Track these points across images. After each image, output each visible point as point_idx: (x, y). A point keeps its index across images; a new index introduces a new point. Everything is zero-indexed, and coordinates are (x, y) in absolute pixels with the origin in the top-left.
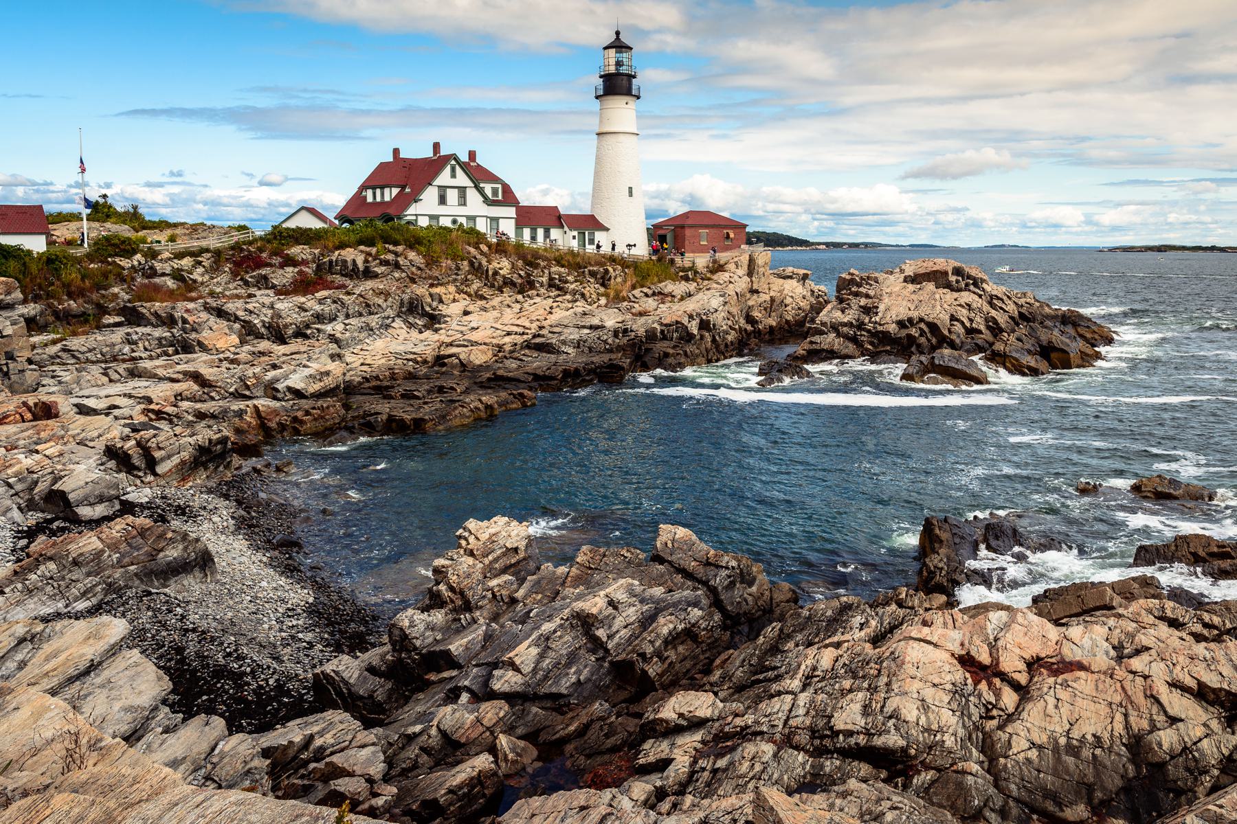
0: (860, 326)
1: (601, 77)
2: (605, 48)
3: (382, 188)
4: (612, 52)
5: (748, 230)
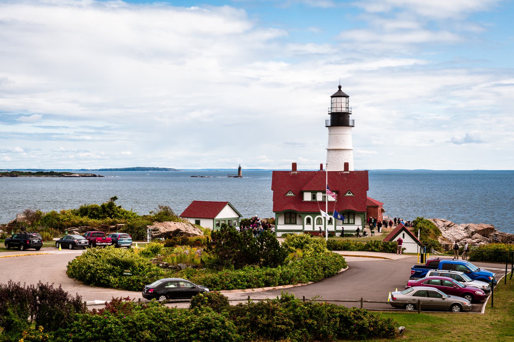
4: (344, 99)
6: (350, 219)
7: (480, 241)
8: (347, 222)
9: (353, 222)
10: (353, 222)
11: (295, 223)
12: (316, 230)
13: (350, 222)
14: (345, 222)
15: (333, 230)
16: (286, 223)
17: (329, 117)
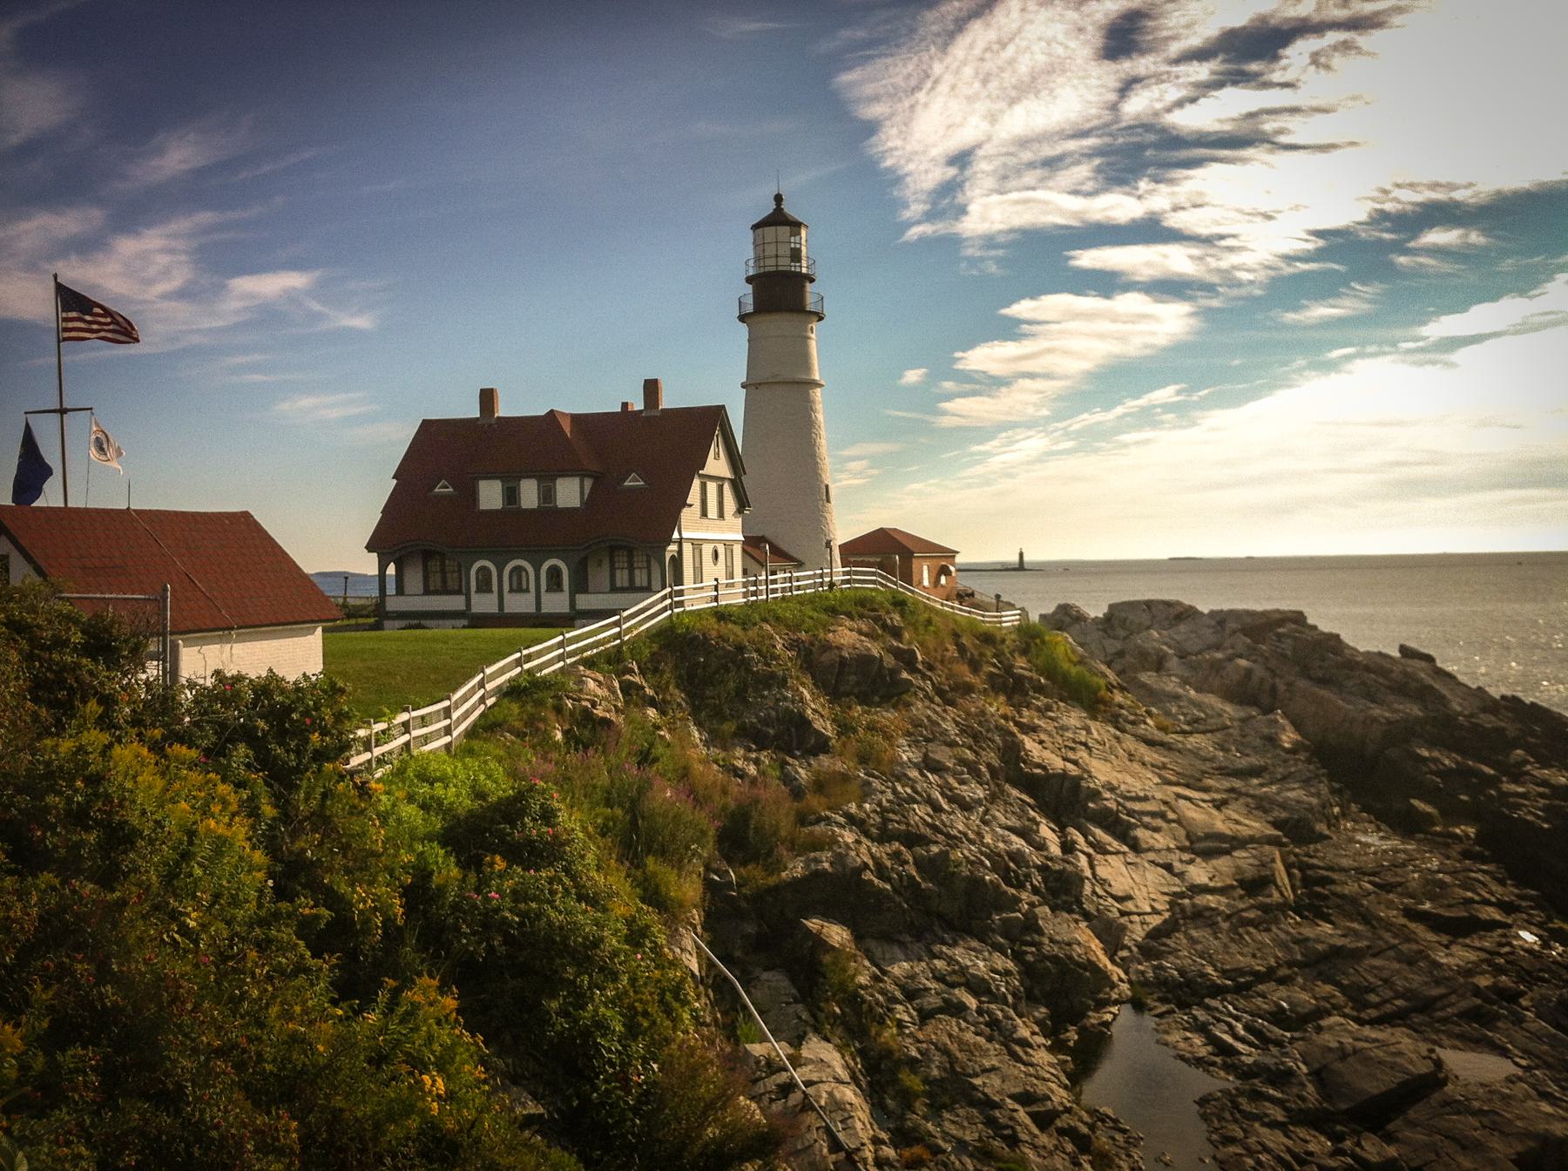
0: (1449, 720)
1: (749, 280)
2: (755, 227)
3: (547, 480)
4: (784, 231)
5: (959, 559)
6: (637, 572)
7: (1241, 656)
8: (626, 584)
9: (645, 584)
13: (638, 583)
14: (619, 584)
15: (566, 609)
16: (427, 592)
17: (749, 289)
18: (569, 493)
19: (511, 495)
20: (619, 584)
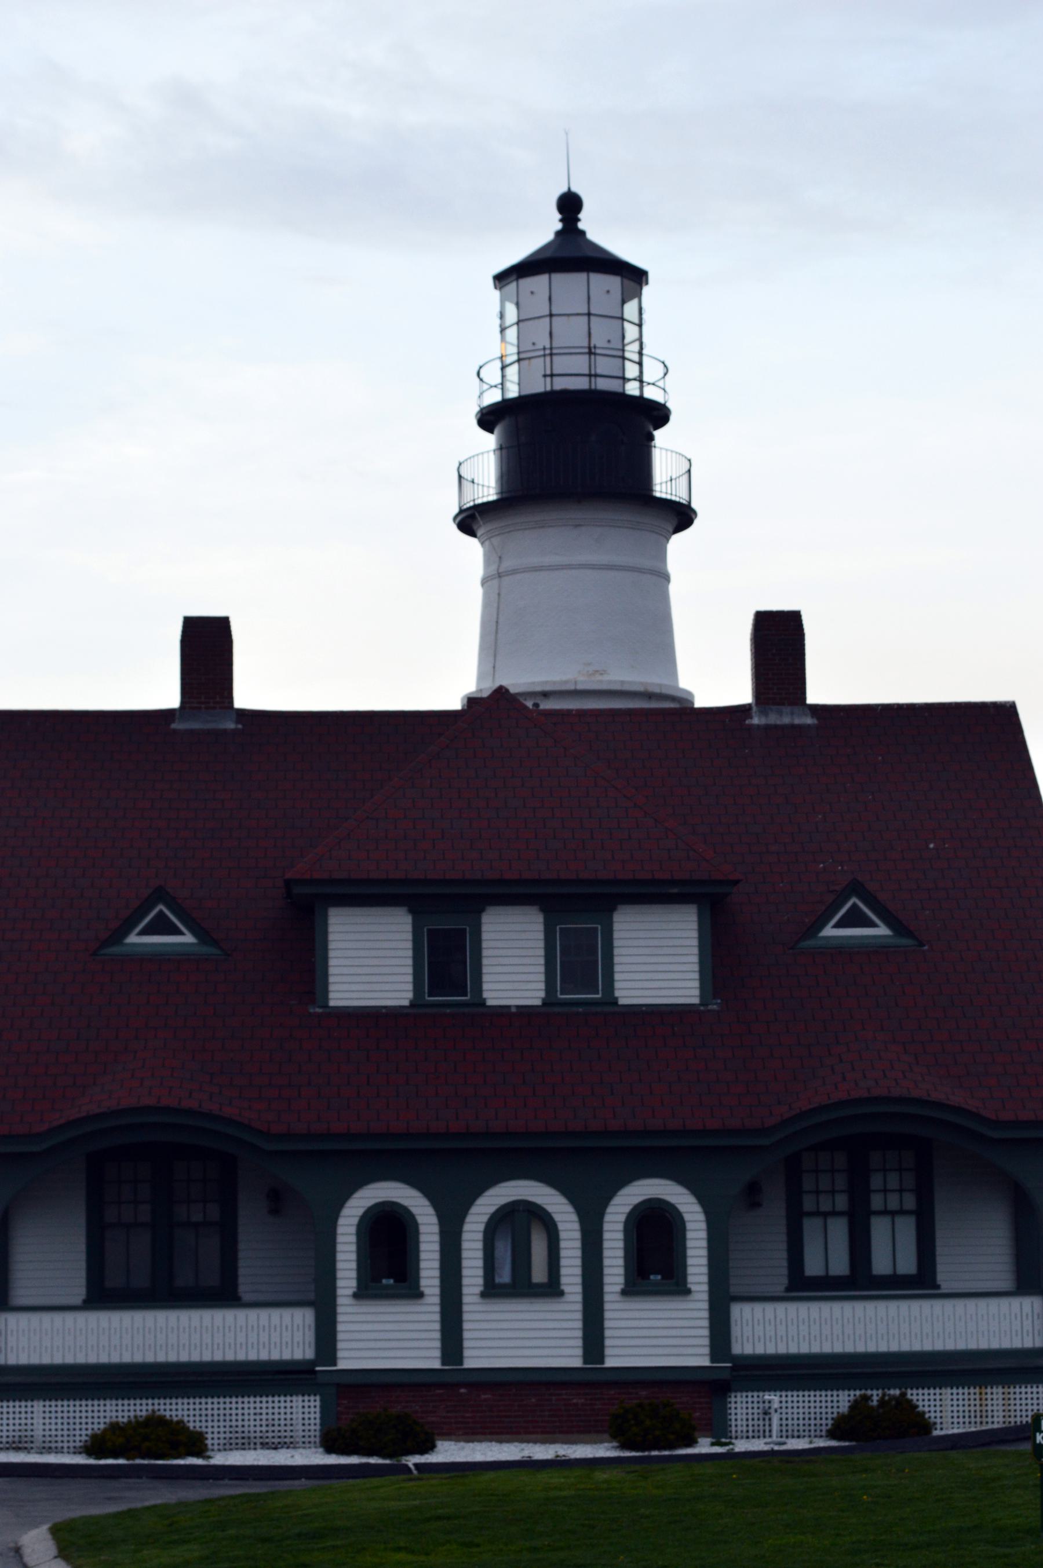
6: (880, 1228)
8: (840, 1266)
9: (907, 1265)
10: (907, 1265)
11: (223, 1293)
12: (478, 1356)
13: (881, 1265)
14: (813, 1267)
16: (103, 1294)
18: (657, 961)
19: (447, 962)
20: (813, 1267)
